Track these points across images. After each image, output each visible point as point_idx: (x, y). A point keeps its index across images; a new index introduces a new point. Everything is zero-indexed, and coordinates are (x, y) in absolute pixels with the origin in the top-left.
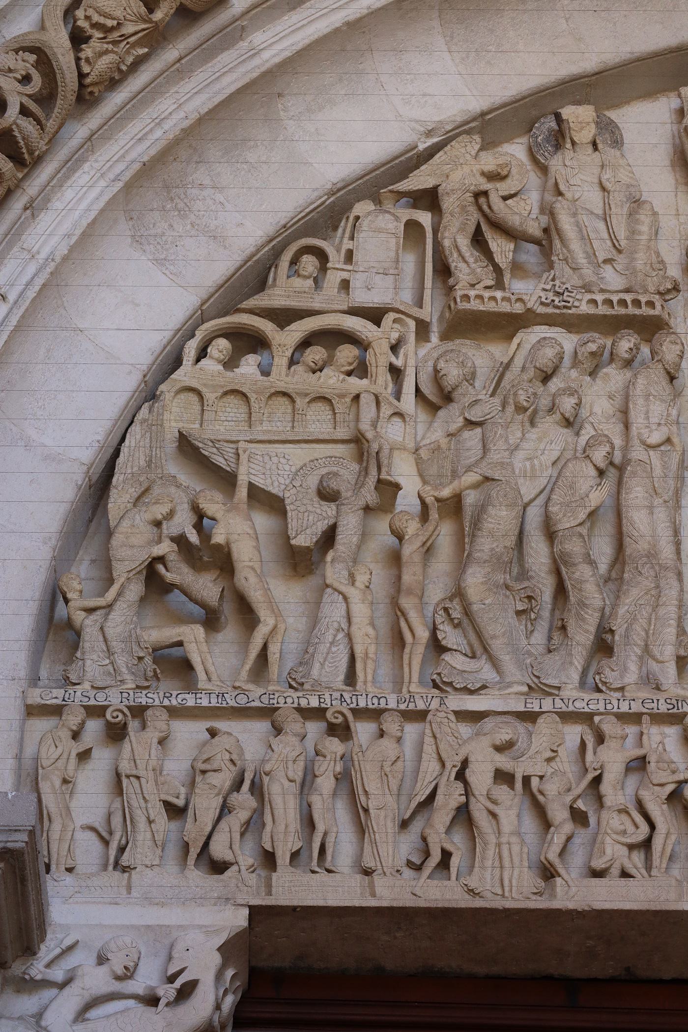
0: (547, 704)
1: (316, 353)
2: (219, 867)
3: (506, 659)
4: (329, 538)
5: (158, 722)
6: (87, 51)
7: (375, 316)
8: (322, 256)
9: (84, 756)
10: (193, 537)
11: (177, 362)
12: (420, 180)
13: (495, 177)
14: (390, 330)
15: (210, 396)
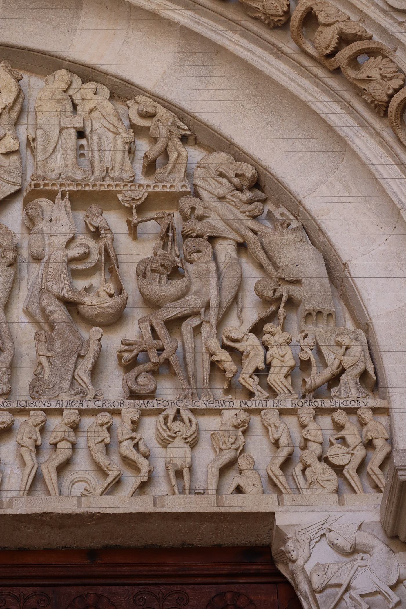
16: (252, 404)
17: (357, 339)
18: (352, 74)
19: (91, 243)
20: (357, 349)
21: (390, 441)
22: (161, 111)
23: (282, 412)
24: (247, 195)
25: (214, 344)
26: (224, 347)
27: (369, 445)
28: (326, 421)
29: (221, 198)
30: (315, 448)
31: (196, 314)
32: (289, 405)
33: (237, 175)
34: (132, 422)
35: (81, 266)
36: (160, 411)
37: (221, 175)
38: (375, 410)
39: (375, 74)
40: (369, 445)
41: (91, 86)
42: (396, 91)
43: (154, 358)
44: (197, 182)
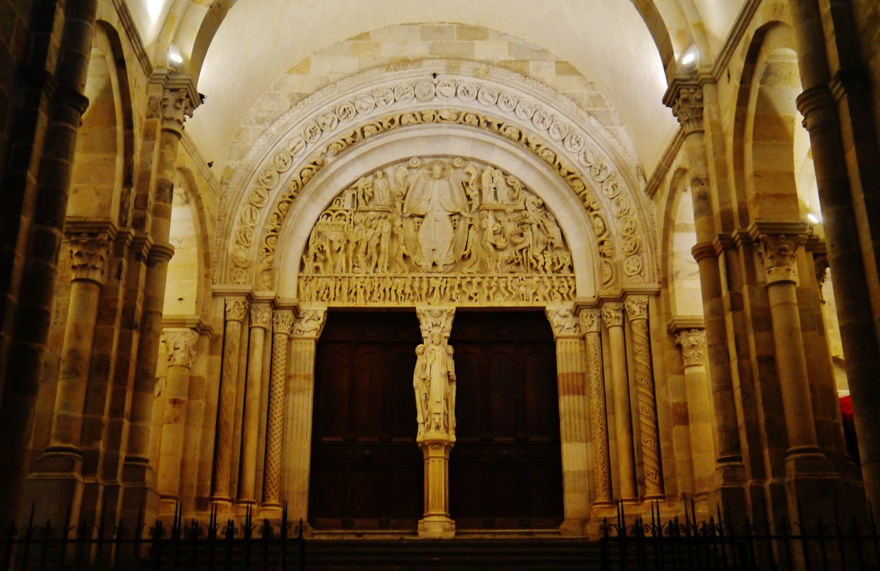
0: (368, 275)
1: (339, 217)
2: (324, 301)
3: (363, 268)
4: (340, 249)
5: (315, 279)
6: (303, 180)
7: (347, 211)
8: (340, 200)
9: (306, 284)
10: (321, 249)
11: (318, 220)
12: (354, 186)
13: (366, 185)
14: (349, 213)
15: (324, 225)
16: (541, 275)
17: (567, 256)
18: (570, 183)
19: (498, 225)
20: (568, 259)
21: (575, 286)
22: (517, 181)
23: (549, 278)
24: (540, 210)
25: (531, 258)
26: (534, 258)
27: (570, 287)
28: (559, 279)
29: (534, 211)
30: (556, 288)
31: (527, 248)
32: (550, 276)
33: (538, 204)
34: (511, 281)
35: (497, 232)
36: (518, 277)
37: (533, 203)
38: (572, 277)
39: (576, 185)
40: (570, 287)
41: (497, 171)
42: (582, 191)
43: (516, 261)
44: (527, 205)
